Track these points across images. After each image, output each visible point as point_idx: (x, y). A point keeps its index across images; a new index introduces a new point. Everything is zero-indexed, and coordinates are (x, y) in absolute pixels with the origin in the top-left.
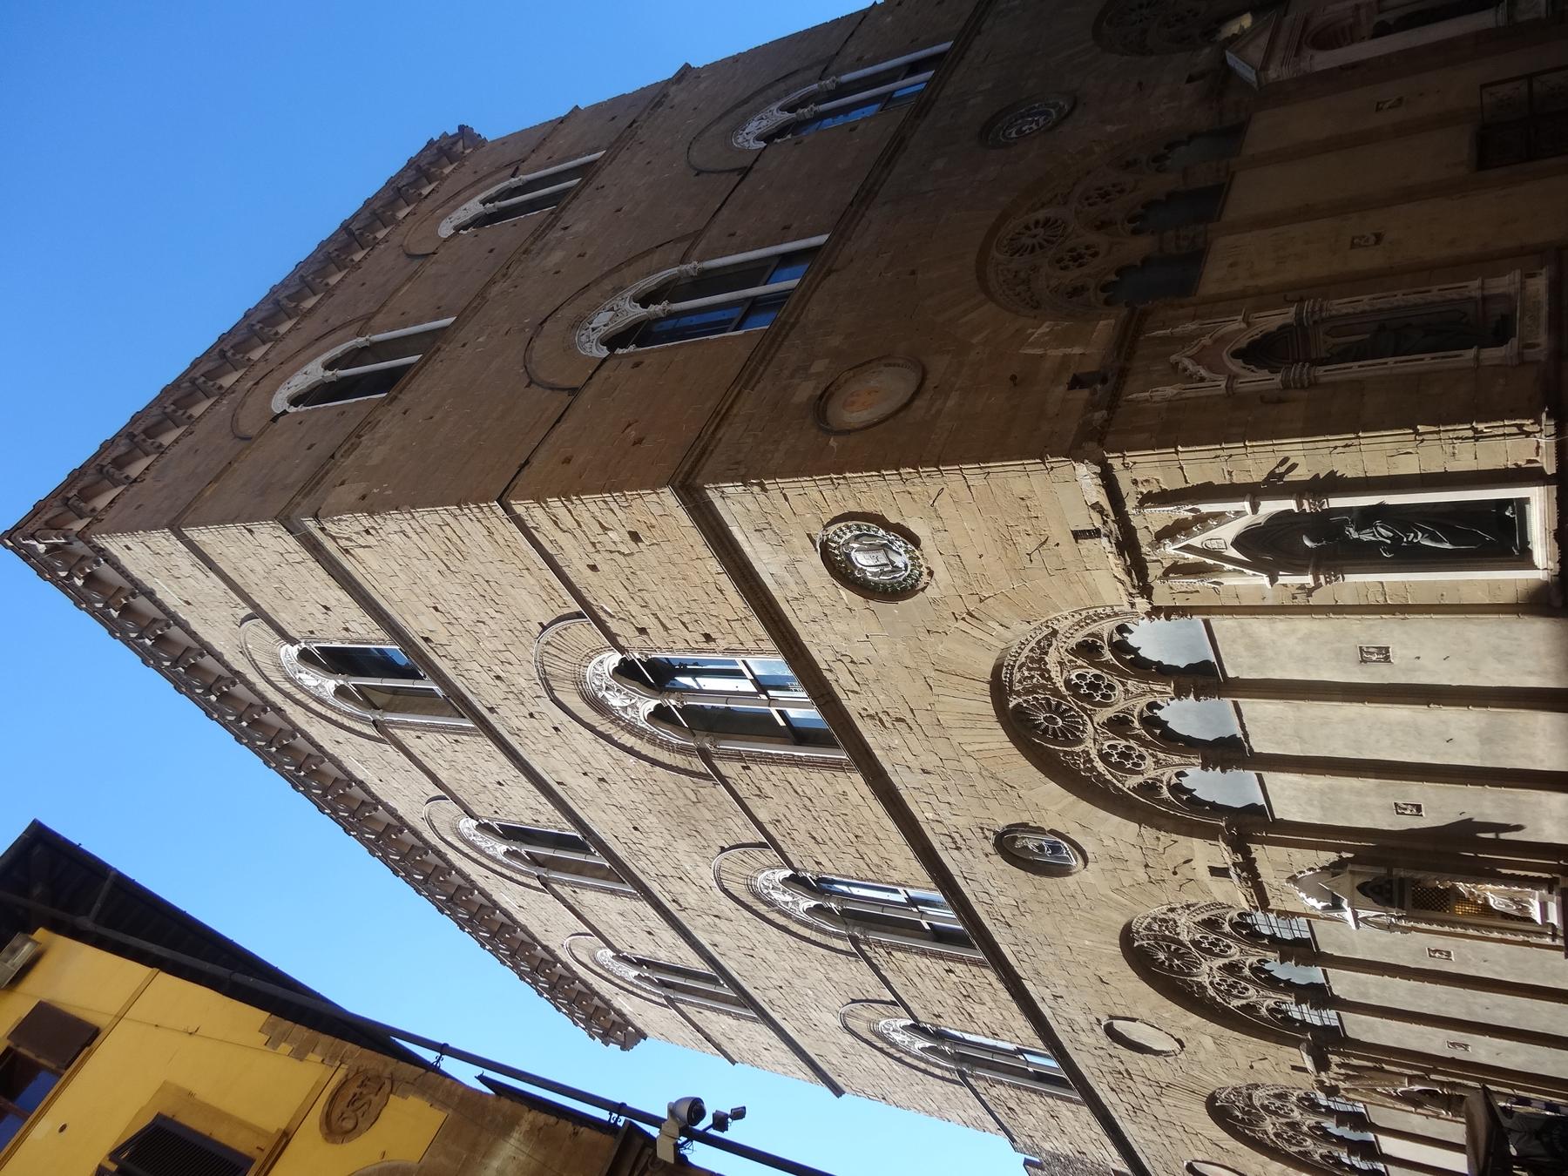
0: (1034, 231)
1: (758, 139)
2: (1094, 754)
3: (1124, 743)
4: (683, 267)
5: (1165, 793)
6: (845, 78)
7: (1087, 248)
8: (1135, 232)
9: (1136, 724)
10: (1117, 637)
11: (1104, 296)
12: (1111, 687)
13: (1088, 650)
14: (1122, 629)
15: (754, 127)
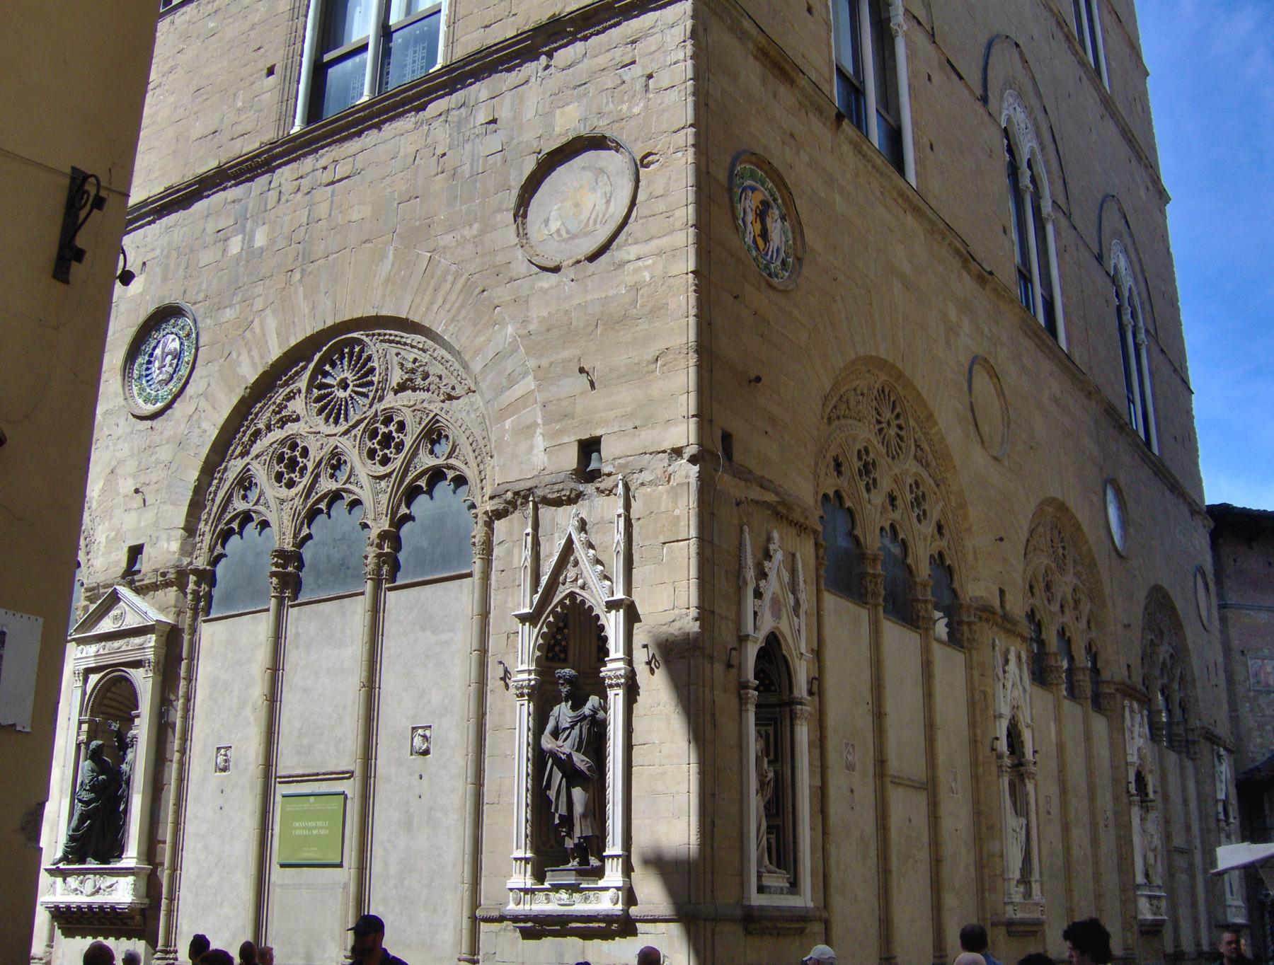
0: (894, 423)
1: (1009, 120)
2: (291, 428)
3: (310, 466)
4: (901, 11)
5: (239, 505)
6: (1050, 229)
7: (875, 480)
8: (882, 529)
9: (334, 486)
10: (451, 474)
11: (832, 495)
12: (385, 461)
13: (433, 435)
14: (460, 481)
15: (1020, 117)
